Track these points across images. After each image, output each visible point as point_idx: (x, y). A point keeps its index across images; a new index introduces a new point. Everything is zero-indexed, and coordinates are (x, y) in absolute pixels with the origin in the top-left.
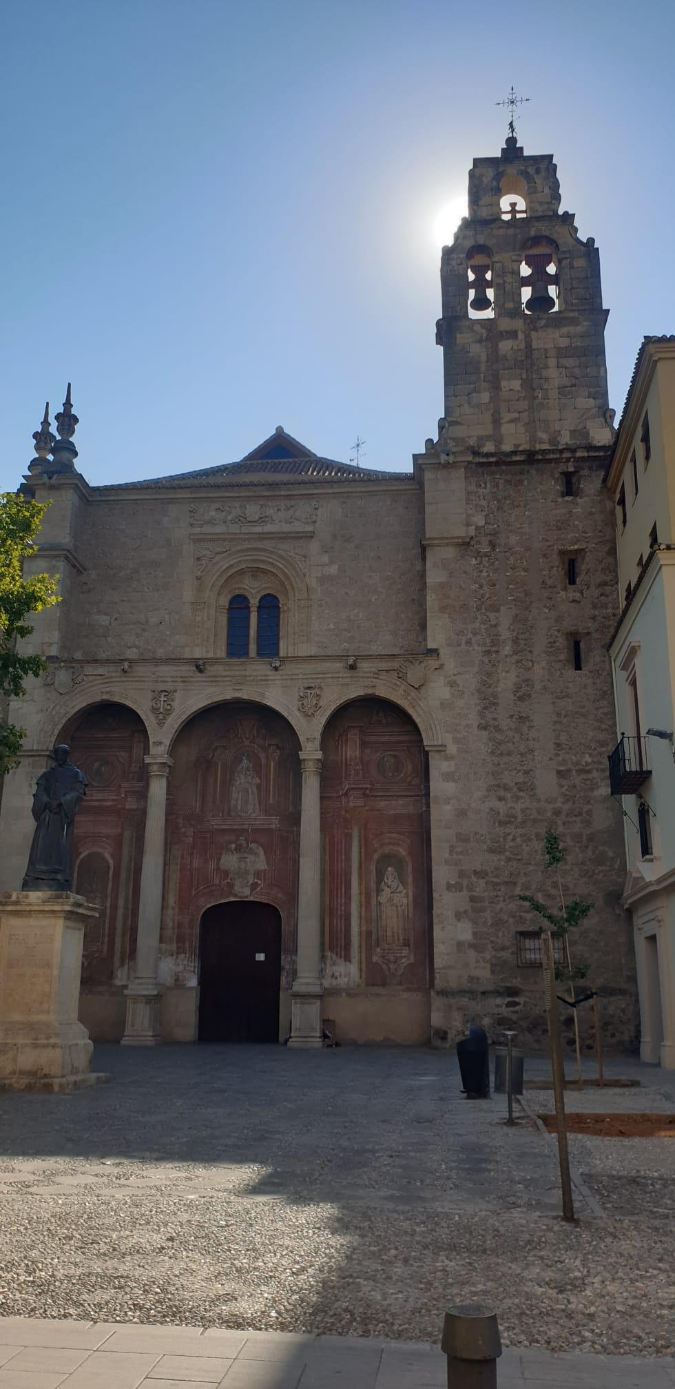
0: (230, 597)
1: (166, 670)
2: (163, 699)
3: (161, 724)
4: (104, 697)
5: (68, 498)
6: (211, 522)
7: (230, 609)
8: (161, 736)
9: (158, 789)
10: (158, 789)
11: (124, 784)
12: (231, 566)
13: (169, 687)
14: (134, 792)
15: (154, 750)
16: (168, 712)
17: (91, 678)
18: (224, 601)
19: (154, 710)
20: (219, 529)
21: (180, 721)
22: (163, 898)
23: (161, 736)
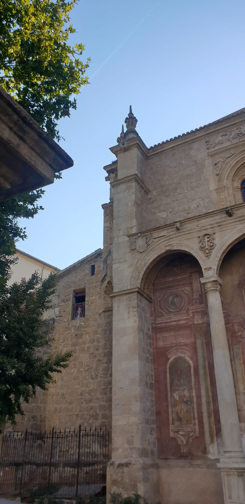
0: (240, 181)
1: (205, 222)
2: (206, 240)
3: (208, 256)
4: (168, 248)
5: (135, 152)
6: (221, 143)
7: (242, 188)
8: (210, 265)
9: (214, 300)
10: (214, 300)
11: (191, 308)
12: (238, 162)
13: (210, 231)
14: (198, 312)
15: (205, 274)
16: (212, 247)
17: (157, 239)
18: (238, 184)
19: (202, 249)
20: (228, 144)
21: (221, 252)
22: (235, 386)
23: (210, 265)
